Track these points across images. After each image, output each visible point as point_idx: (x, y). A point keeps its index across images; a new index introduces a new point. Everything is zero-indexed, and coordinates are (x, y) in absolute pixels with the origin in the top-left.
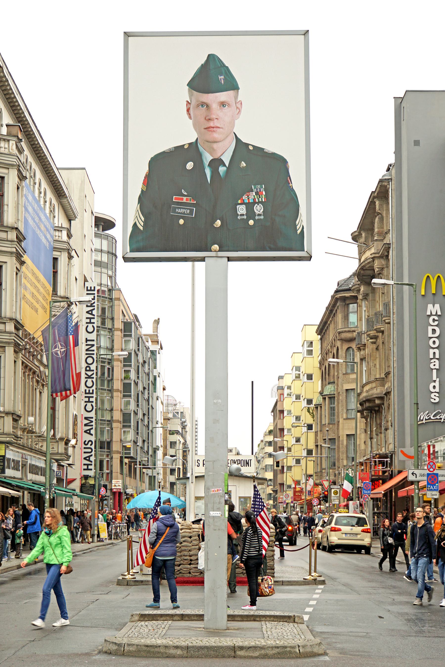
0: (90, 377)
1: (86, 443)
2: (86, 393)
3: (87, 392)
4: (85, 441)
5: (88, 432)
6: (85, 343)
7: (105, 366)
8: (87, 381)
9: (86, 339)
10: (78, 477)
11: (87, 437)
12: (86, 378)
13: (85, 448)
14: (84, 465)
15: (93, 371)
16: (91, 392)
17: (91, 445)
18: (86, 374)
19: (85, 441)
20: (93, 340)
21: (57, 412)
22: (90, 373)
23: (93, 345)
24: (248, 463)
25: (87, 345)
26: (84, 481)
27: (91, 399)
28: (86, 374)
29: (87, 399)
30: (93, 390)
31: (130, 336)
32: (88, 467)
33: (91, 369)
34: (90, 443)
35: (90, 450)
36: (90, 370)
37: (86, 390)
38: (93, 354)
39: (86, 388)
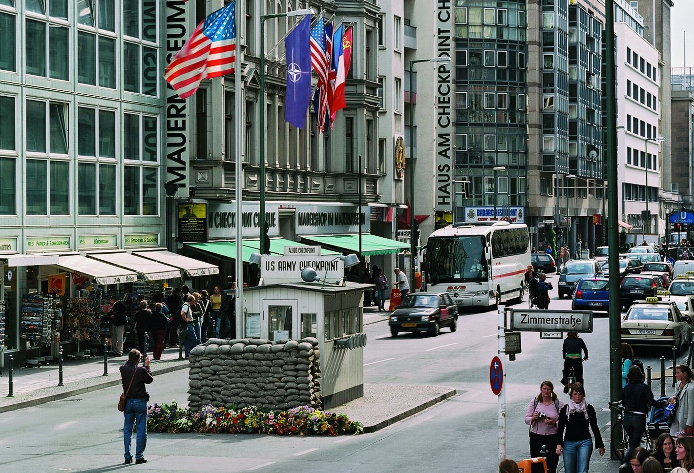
0: (444, 80)
1: (441, 168)
2: (440, 102)
3: (442, 100)
4: (440, 166)
5: (444, 154)
6: (437, 36)
7: (515, 52)
8: (441, 86)
9: (439, 29)
10: (432, 213)
11: (444, 161)
12: (439, 82)
13: (439, 175)
14: (439, 197)
15: (449, 72)
16: (446, 100)
17: (448, 171)
18: (439, 76)
19: (440, 166)
20: (448, 31)
21: (355, 140)
22: (444, 75)
23: (448, 38)
24: (333, 266)
25: (440, 38)
26: (439, 219)
27: (447, 111)
28: (439, 76)
29: (441, 111)
30: (449, 98)
31: (552, 9)
32: (444, 200)
34: (446, 168)
35: (446, 178)
36: (445, 71)
37: (439, 98)
38: (449, 50)
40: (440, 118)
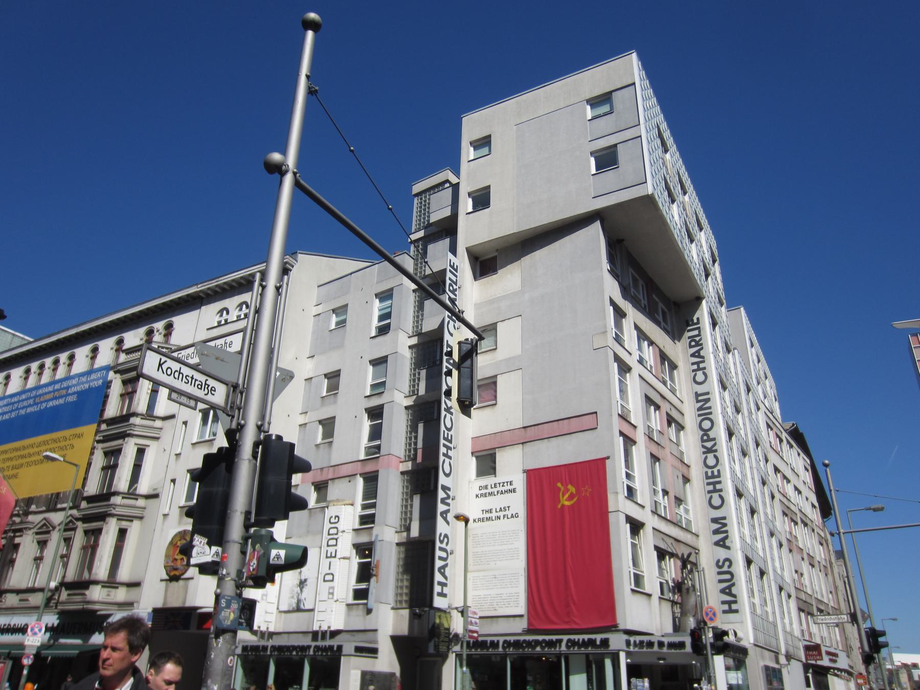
1: (720, 564)
2: (708, 477)
3: (710, 474)
9: (696, 393)
12: (704, 453)
13: (719, 573)
16: (716, 473)
17: (729, 566)
19: (718, 561)
25: (698, 401)
28: (703, 447)
30: (719, 471)
33: (711, 437)
34: (727, 563)
35: (728, 577)
36: (709, 440)
37: (706, 473)
38: (711, 413)
39: (706, 469)
40: (711, 497)
